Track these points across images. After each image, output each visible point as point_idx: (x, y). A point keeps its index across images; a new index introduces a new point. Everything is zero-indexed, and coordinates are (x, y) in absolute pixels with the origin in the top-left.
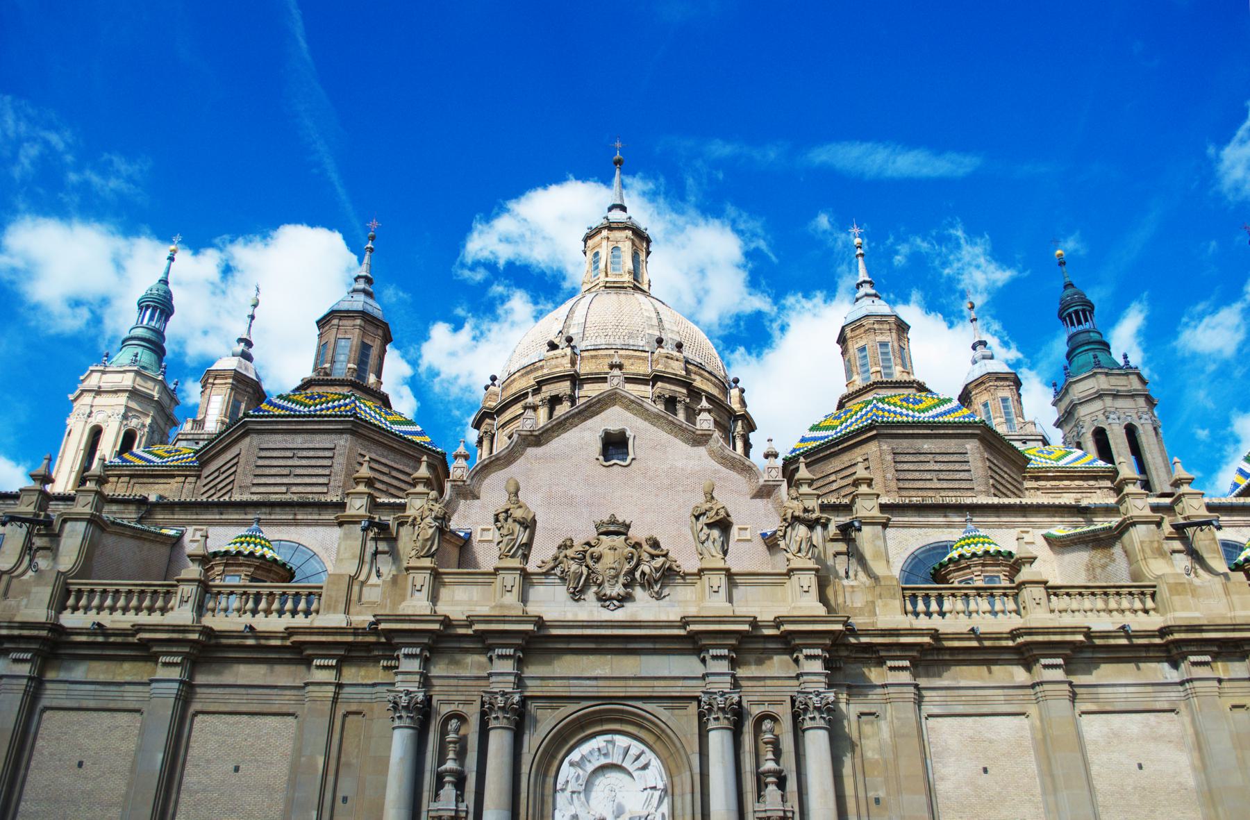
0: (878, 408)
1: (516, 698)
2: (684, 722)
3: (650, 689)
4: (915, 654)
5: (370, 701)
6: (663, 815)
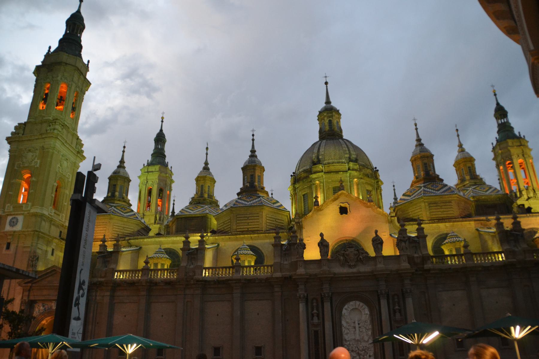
0: (424, 190)
1: (330, 294)
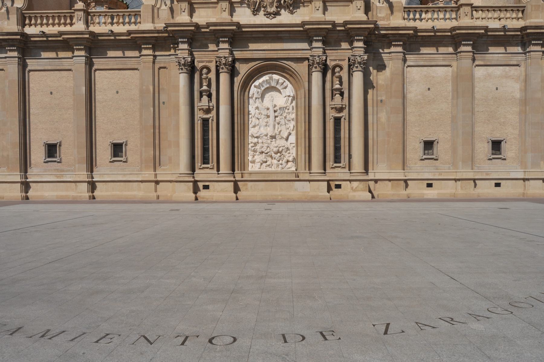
1: (230, 59)
3: (288, 55)
4: (406, 39)
5: (169, 62)
6: (293, 107)
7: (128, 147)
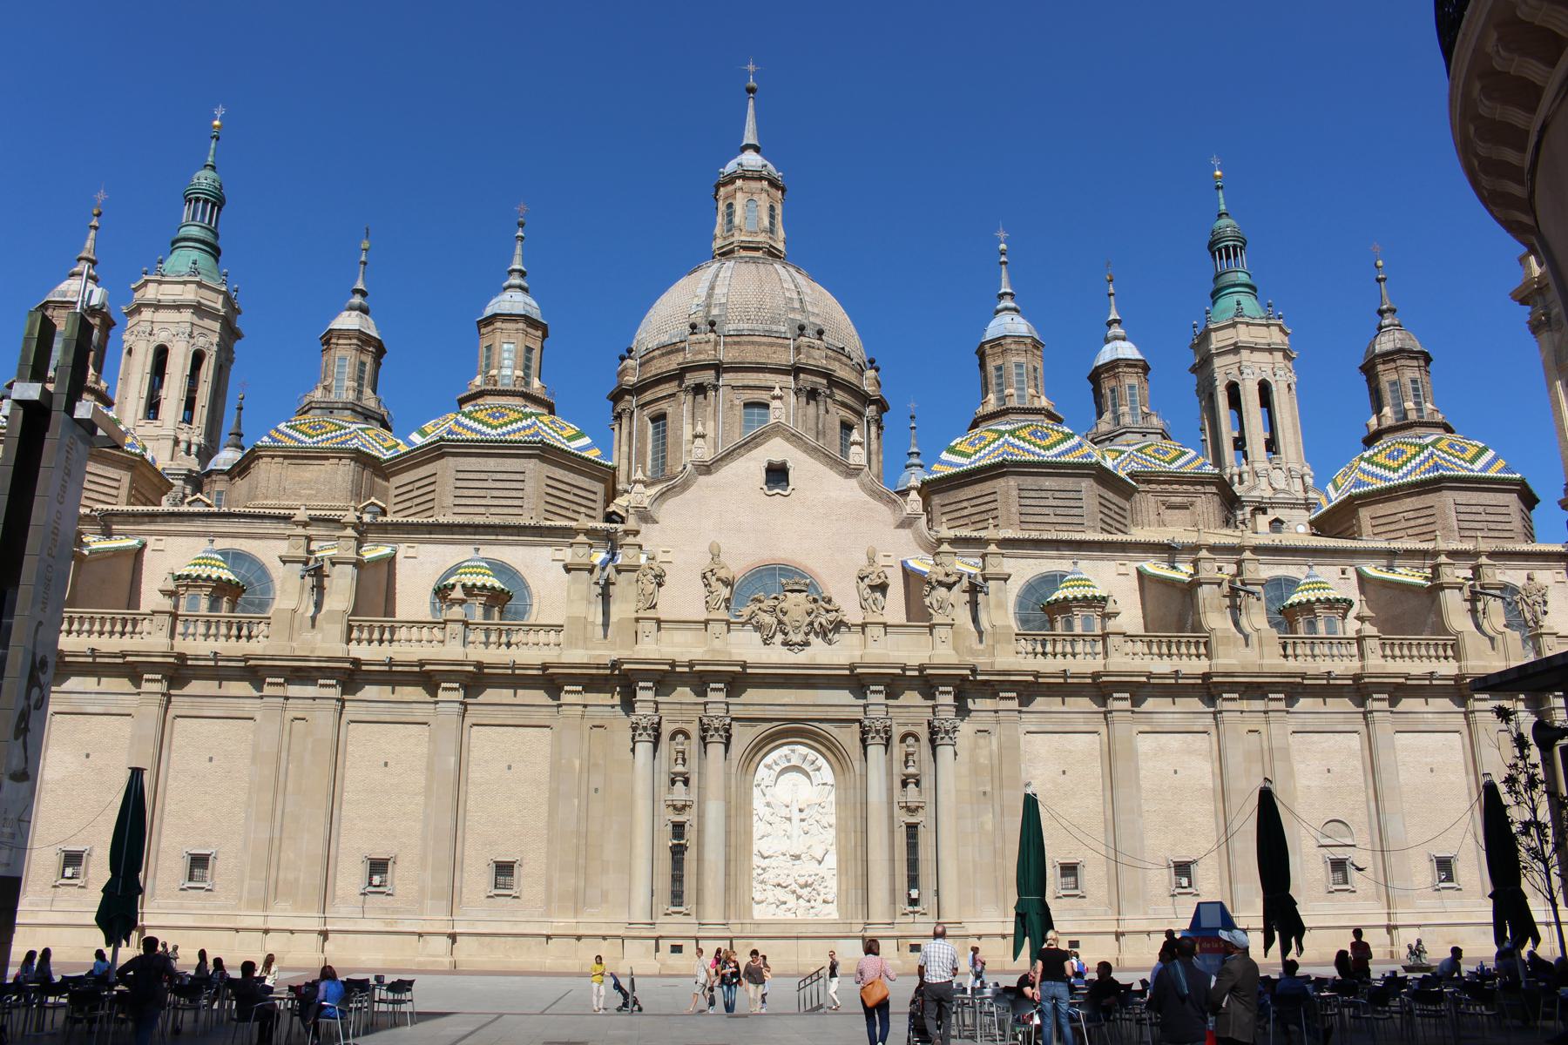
0: (1009, 443)
2: (848, 738)
4: (1022, 688)
7: (526, 869)
